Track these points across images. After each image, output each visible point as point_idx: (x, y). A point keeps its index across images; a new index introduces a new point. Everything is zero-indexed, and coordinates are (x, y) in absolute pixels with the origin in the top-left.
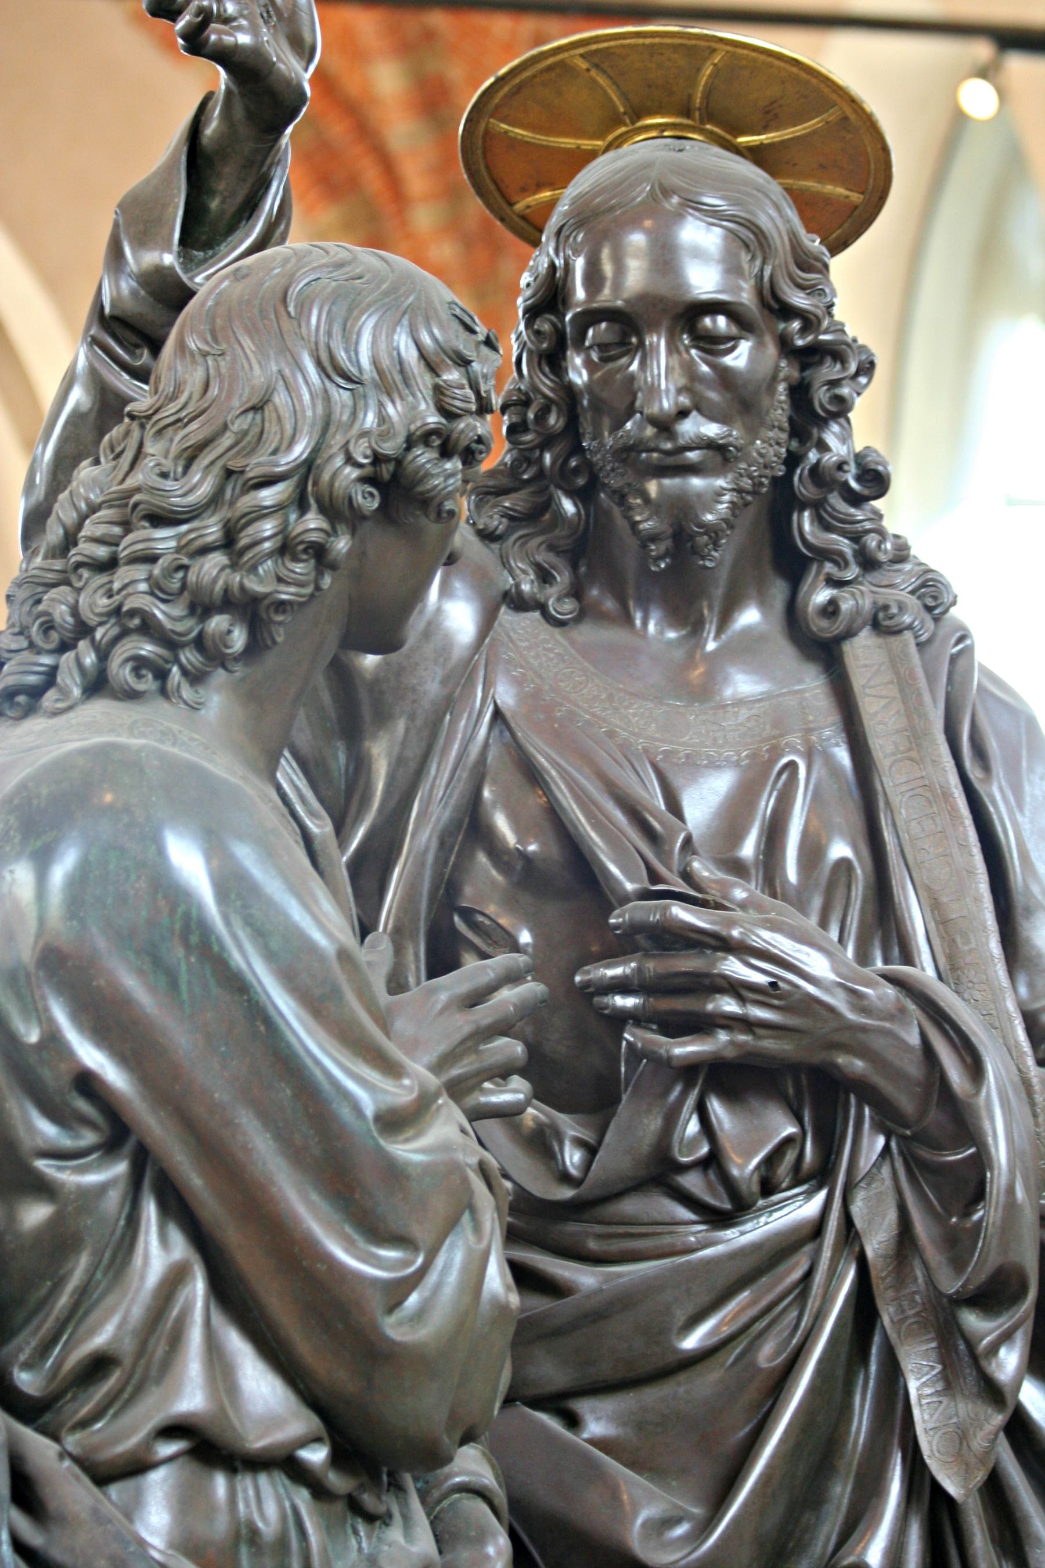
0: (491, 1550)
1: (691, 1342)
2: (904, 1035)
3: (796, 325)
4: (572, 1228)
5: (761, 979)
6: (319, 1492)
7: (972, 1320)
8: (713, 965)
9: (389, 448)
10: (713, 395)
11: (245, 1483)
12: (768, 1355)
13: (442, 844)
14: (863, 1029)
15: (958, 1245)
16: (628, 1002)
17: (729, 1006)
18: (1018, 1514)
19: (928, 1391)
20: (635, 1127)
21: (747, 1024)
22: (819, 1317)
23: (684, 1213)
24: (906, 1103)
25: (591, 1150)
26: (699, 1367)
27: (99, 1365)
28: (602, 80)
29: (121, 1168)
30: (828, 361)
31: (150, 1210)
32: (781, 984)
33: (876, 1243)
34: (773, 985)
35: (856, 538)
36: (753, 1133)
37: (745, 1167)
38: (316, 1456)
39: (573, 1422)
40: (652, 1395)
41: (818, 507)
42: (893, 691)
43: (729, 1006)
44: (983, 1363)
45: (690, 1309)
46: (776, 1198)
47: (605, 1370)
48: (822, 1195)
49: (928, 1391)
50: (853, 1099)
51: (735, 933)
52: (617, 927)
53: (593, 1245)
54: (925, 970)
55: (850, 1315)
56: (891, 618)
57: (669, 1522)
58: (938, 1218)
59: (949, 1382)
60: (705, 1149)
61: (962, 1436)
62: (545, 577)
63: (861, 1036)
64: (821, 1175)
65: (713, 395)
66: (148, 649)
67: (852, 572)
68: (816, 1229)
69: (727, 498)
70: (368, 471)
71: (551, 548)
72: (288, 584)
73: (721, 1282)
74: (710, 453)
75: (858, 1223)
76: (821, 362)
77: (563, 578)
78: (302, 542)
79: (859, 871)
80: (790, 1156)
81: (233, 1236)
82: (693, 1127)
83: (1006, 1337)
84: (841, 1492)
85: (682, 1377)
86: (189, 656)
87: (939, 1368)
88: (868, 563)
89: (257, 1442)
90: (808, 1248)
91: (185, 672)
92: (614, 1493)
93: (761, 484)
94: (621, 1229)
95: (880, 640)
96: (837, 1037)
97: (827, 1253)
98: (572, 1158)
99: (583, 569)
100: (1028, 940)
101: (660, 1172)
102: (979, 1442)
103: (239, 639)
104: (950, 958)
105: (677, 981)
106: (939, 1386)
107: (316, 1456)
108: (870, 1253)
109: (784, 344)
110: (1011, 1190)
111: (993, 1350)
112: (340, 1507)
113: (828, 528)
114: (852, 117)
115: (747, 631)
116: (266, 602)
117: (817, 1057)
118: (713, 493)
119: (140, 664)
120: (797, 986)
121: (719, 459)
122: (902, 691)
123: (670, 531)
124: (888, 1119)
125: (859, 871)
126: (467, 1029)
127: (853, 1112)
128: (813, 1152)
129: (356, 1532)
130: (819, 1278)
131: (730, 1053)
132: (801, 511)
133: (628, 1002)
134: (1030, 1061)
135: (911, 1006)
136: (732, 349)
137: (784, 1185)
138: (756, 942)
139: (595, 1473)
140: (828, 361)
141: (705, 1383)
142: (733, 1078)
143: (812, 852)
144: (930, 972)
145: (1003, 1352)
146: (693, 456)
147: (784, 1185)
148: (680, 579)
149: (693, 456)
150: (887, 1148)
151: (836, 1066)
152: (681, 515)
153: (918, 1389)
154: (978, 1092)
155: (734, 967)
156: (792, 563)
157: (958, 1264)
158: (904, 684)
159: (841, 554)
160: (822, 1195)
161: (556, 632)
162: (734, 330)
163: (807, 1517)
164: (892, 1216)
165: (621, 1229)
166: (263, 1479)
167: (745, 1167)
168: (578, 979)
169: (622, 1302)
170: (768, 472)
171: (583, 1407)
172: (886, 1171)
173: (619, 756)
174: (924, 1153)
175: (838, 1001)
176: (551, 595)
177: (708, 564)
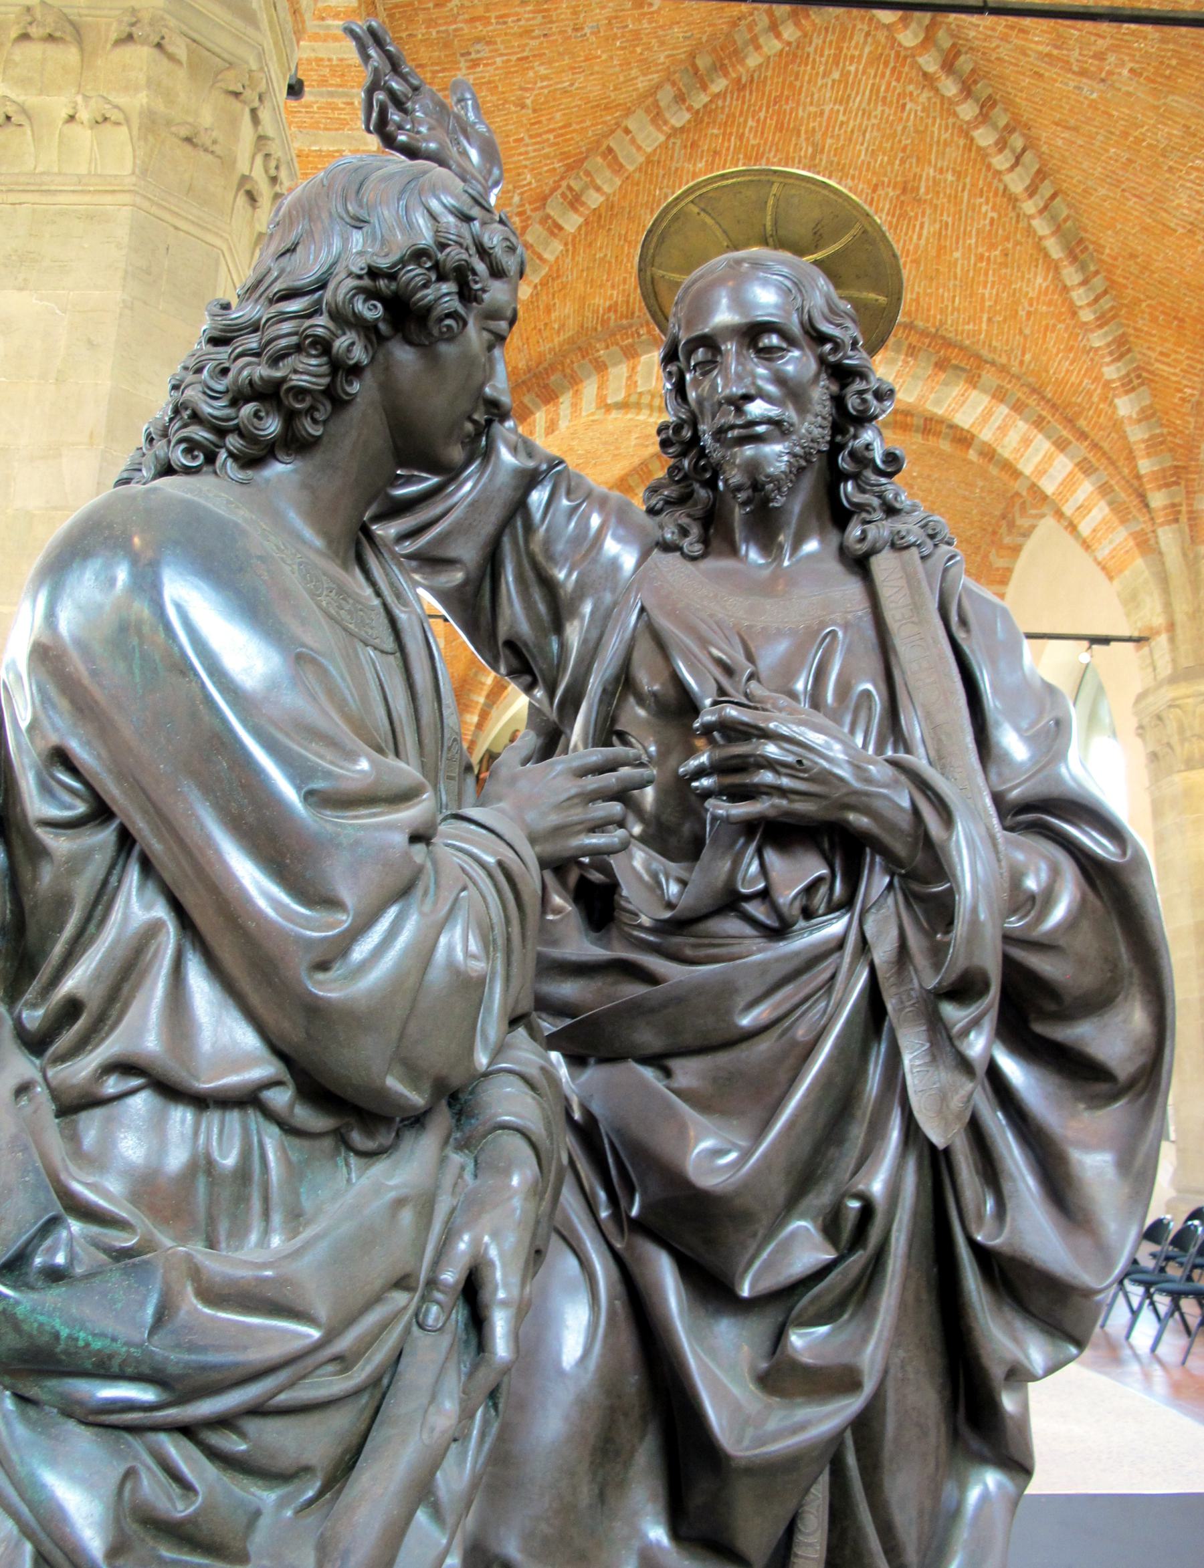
0: (515, 1181)
1: (746, 1021)
2: (897, 799)
3: (828, 347)
4: (677, 940)
5: (790, 759)
6: (289, 1129)
7: (951, 1011)
8: (757, 748)
9: (383, 263)
10: (771, 388)
11: (213, 1118)
12: (802, 1032)
13: (604, 691)
14: (867, 794)
15: (937, 953)
16: (706, 782)
17: (767, 777)
18: (995, 1155)
19: (918, 1062)
20: (714, 869)
21: (782, 792)
22: (840, 1005)
23: (748, 930)
24: (900, 848)
25: (683, 883)
26: (756, 1040)
27: (72, 1008)
28: (709, 221)
29: (106, 836)
30: (858, 380)
31: (134, 875)
32: (805, 762)
33: (883, 952)
34: (799, 762)
35: (880, 496)
36: (794, 873)
37: (787, 895)
38: (280, 1098)
39: (668, 1073)
40: (723, 1059)
41: (855, 477)
42: (903, 582)
43: (767, 777)
44: (957, 1043)
45: (749, 997)
46: (814, 921)
47: (688, 1039)
48: (846, 919)
49: (918, 1062)
50: (868, 850)
51: (772, 725)
52: (697, 729)
53: (689, 952)
54: (919, 760)
55: (865, 1003)
56: (903, 538)
57: (719, 1153)
58: (929, 934)
59: (934, 1055)
60: (761, 885)
61: (943, 1097)
62: (684, 532)
63: (864, 799)
64: (847, 904)
65: (771, 388)
66: (200, 434)
67: (878, 515)
68: (840, 944)
69: (786, 458)
70: (366, 282)
71: (689, 516)
72: (302, 373)
73: (771, 978)
74: (771, 427)
75: (868, 935)
76: (853, 382)
77: (695, 531)
78: (308, 336)
79: (877, 698)
80: (823, 889)
81: (189, 900)
82: (754, 867)
83: (975, 1023)
84: (857, 1133)
85: (744, 1046)
86: (233, 441)
87: (927, 1045)
88: (891, 511)
89: (206, 1084)
90: (837, 955)
91: (231, 454)
92: (682, 1129)
93: (811, 454)
94: (706, 941)
95: (896, 554)
96: (846, 800)
97: (847, 959)
98: (673, 889)
99: (712, 531)
100: (998, 743)
101: (731, 901)
102: (956, 1102)
103: (272, 426)
104: (938, 751)
105: (734, 762)
106: (927, 1059)
107: (280, 1098)
108: (877, 961)
109: (822, 360)
110: (974, 910)
111: (965, 1033)
112: (328, 1143)
113: (863, 491)
114: (869, 229)
115: (810, 556)
116: (285, 387)
117: (833, 816)
118: (776, 455)
119: (191, 446)
120: (816, 763)
121: (777, 433)
122: (908, 582)
123: (749, 483)
124: (893, 863)
125: (877, 698)
126: (573, 791)
127: (868, 859)
128: (842, 889)
129: (347, 1165)
130: (841, 977)
131: (772, 813)
132: (846, 481)
133: (706, 782)
134: (995, 821)
135: (903, 778)
136: (782, 357)
137: (821, 912)
138: (784, 730)
139: (671, 1113)
140: (858, 380)
141: (763, 1047)
142: (779, 833)
143: (844, 689)
144: (924, 762)
145: (972, 1035)
146: (761, 429)
147: (821, 912)
148: (765, 524)
149: (761, 429)
150: (890, 886)
151: (847, 822)
152: (753, 468)
153: (911, 1061)
154: (950, 838)
155: (771, 750)
156: (840, 516)
157: (937, 966)
158: (911, 580)
159: (870, 505)
160: (846, 919)
161: (689, 566)
162: (784, 345)
163: (832, 1152)
164: (894, 933)
165: (706, 941)
166: (234, 1118)
167: (787, 895)
168: (681, 770)
169: (700, 988)
170: (815, 445)
171: (676, 1064)
172: (890, 901)
173: (715, 627)
174: (916, 887)
175: (844, 772)
176: (685, 543)
177: (776, 505)
